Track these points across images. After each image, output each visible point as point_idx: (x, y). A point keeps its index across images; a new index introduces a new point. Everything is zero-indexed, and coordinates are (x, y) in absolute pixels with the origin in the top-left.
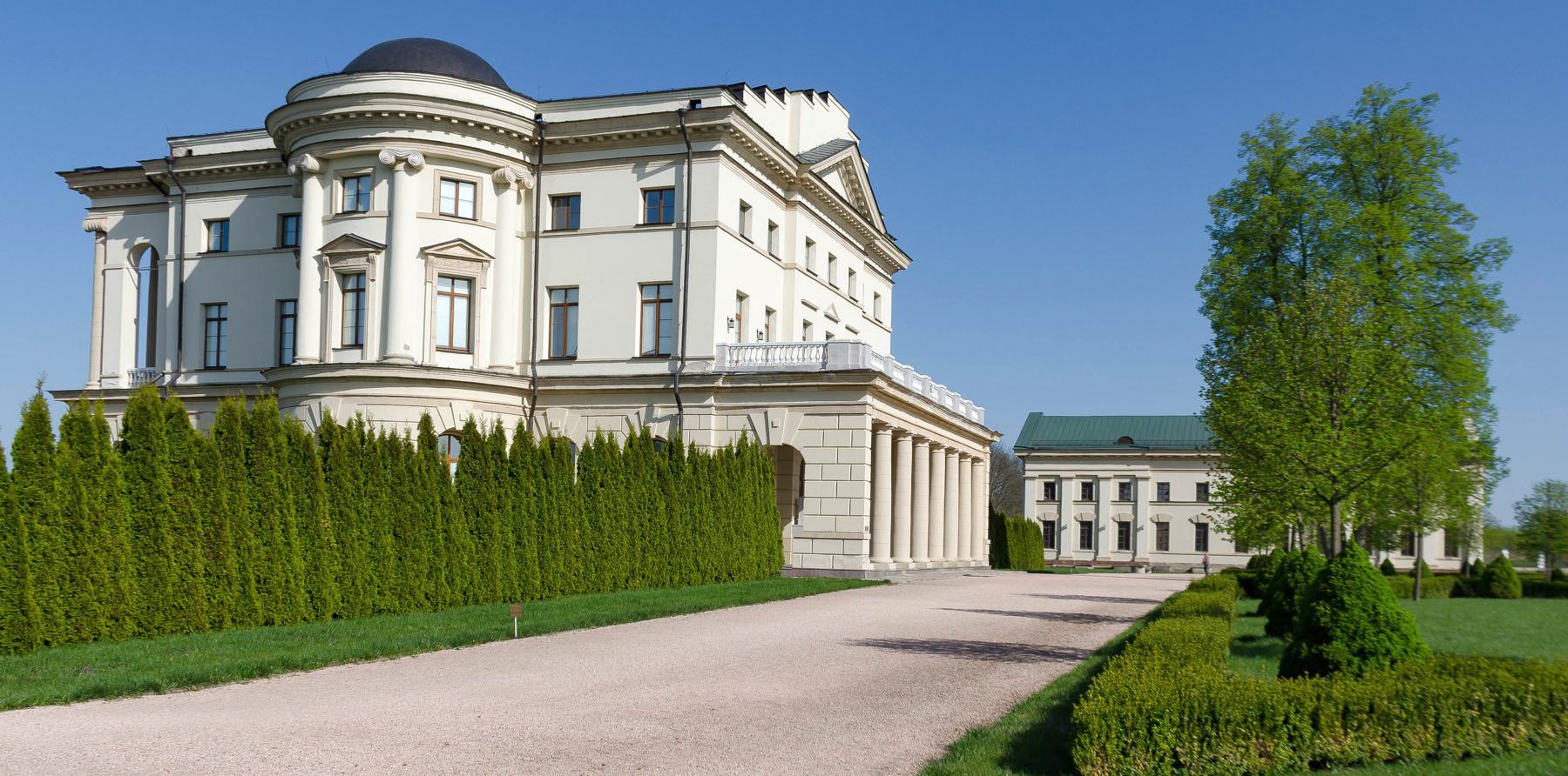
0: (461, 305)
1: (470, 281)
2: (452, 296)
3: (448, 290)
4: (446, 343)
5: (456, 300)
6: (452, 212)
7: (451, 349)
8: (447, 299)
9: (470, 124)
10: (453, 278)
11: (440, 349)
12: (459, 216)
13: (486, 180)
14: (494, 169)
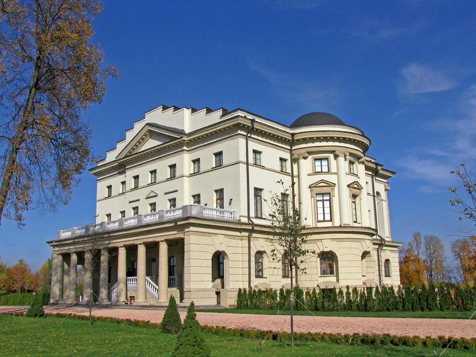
0: (327, 204)
1: (329, 194)
2: (323, 201)
3: (322, 199)
5: (325, 202)
6: (320, 171)
7: (324, 221)
8: (322, 202)
9: (321, 138)
10: (323, 194)
11: (319, 221)
12: (323, 171)
13: (331, 156)
14: (334, 151)
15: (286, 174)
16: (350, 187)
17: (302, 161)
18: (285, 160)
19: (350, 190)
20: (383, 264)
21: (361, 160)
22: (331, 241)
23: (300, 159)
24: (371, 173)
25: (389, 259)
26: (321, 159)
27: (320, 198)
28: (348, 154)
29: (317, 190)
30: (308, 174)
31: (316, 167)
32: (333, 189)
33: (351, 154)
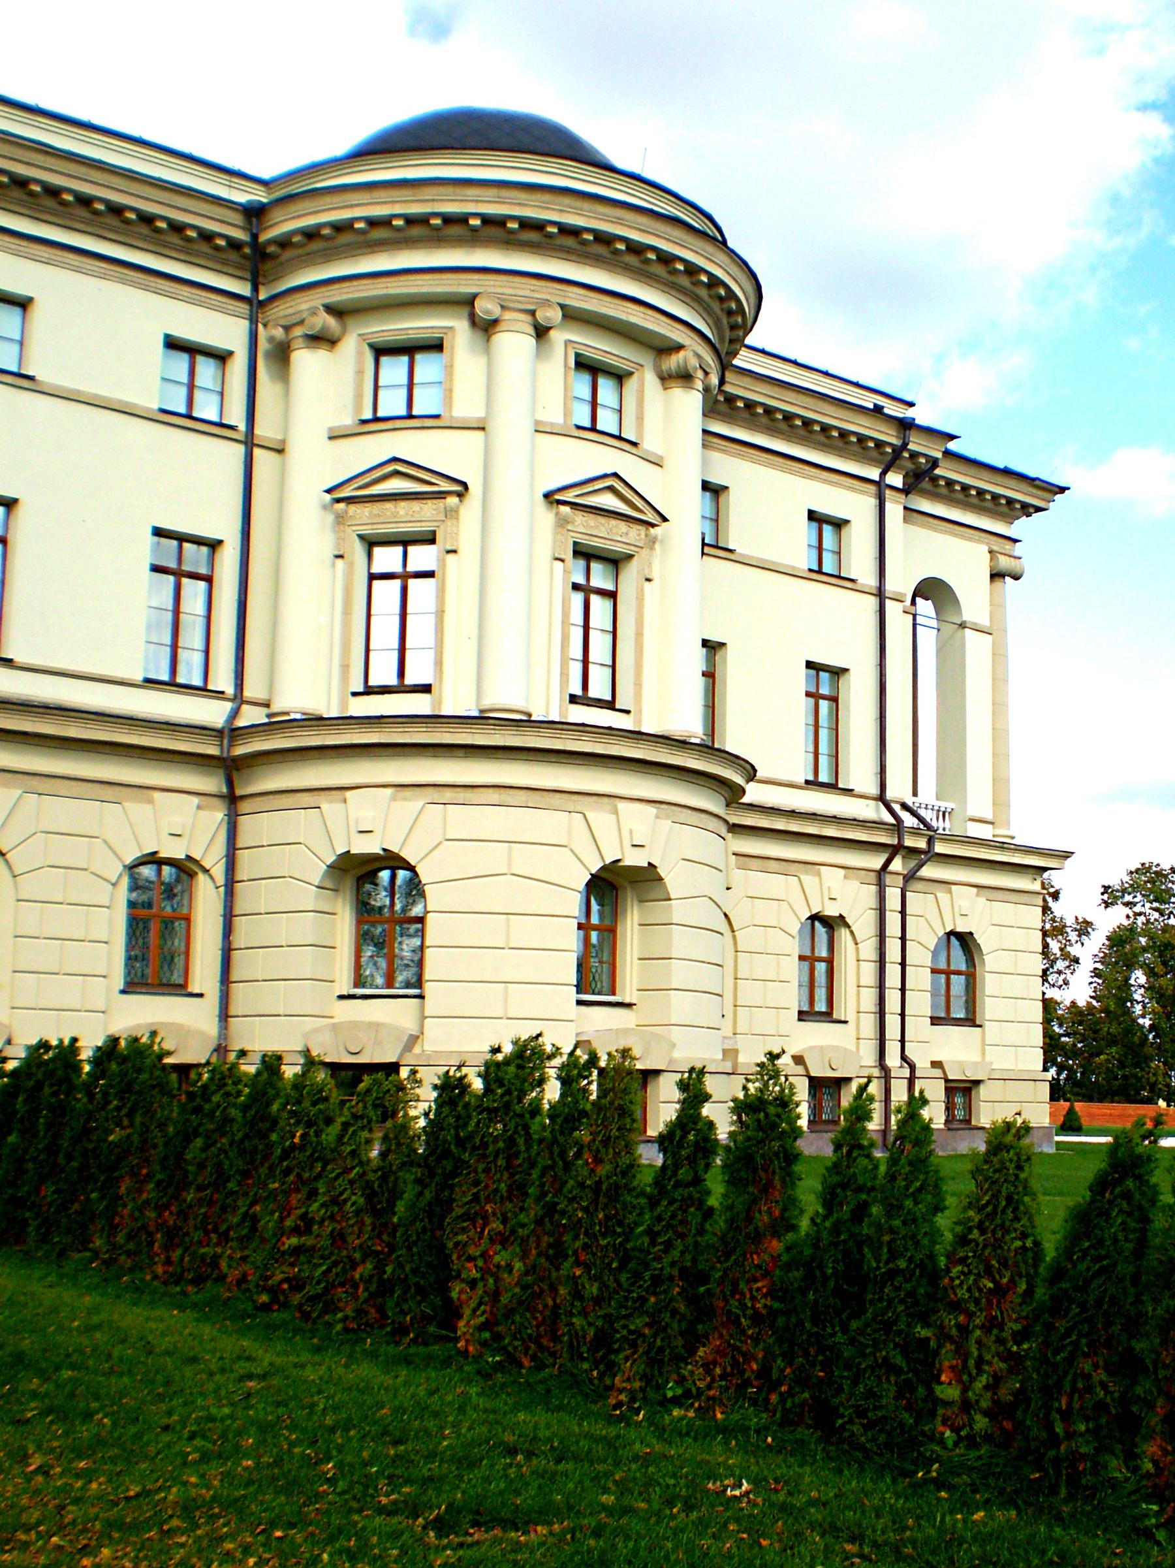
4: (393, 681)
6: (403, 412)
7: (402, 688)
12: (415, 413)
13: (457, 328)
15: (220, 428)
16: (559, 502)
17: (305, 360)
18: (222, 357)
19: (562, 522)
20: (920, 956)
21: (673, 362)
22: (394, 798)
23: (294, 345)
24: (874, 473)
25: (971, 934)
26: (409, 349)
27: (387, 559)
28: (556, 315)
29: (367, 518)
30: (331, 429)
31: (381, 393)
32: (452, 514)
33: (571, 316)
